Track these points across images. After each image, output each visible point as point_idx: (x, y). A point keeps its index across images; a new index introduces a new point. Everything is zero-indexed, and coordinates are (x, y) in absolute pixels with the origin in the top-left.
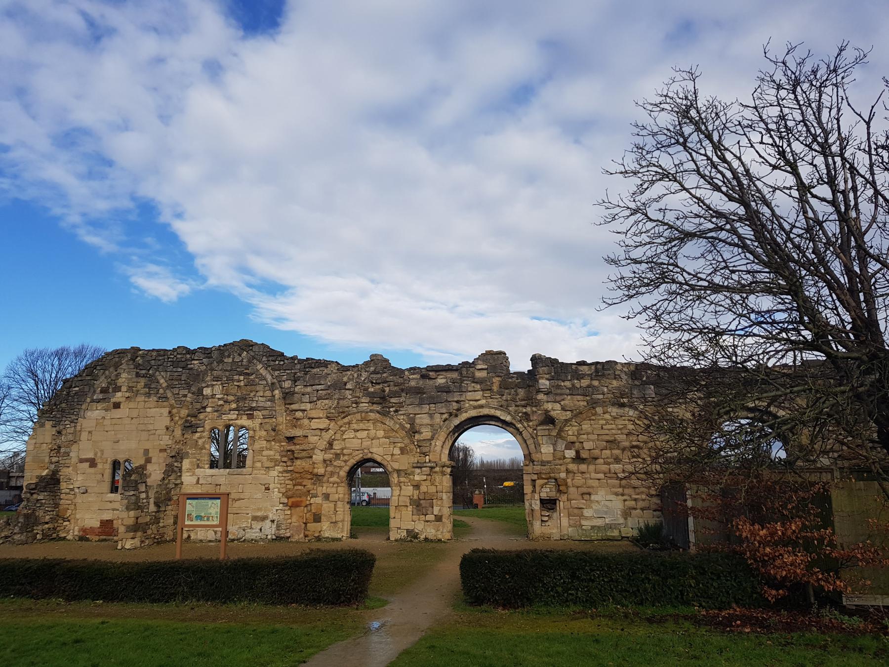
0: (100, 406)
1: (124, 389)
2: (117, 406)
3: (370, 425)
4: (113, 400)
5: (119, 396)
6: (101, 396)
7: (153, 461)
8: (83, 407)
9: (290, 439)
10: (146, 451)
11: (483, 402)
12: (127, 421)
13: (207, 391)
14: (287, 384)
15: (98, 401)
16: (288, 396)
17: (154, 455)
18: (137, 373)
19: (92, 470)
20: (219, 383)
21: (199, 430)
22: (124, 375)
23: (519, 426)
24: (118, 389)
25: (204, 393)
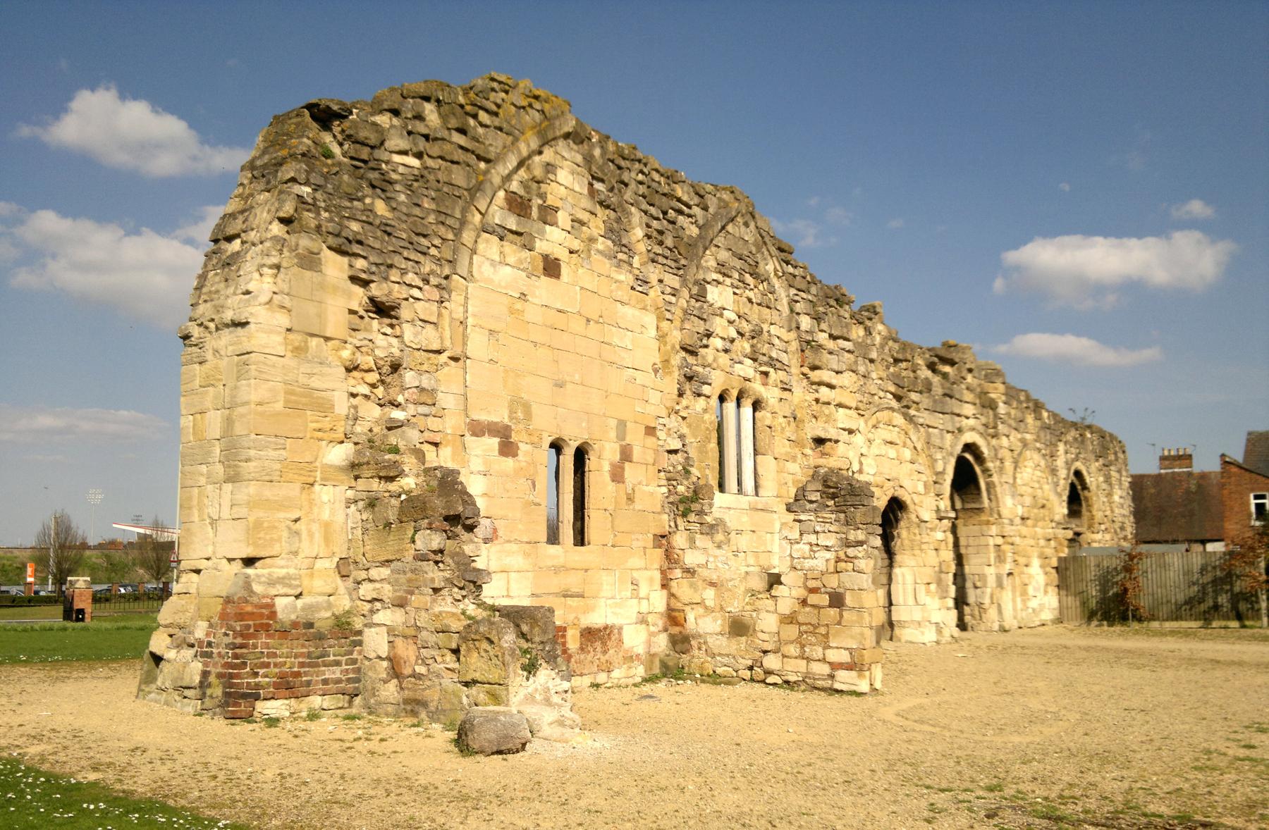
0: (513, 252)
1: (563, 218)
2: (551, 267)
3: (893, 435)
4: (541, 246)
5: (553, 240)
6: (512, 223)
7: (635, 458)
8: (468, 236)
9: (819, 441)
10: (622, 425)
11: (972, 422)
12: (577, 325)
13: (713, 294)
14: (806, 323)
15: (502, 233)
16: (808, 345)
17: (635, 437)
18: (591, 185)
19: (509, 463)
20: (728, 281)
21: (706, 389)
22: (563, 175)
23: (990, 465)
24: (548, 214)
25: (709, 297)
